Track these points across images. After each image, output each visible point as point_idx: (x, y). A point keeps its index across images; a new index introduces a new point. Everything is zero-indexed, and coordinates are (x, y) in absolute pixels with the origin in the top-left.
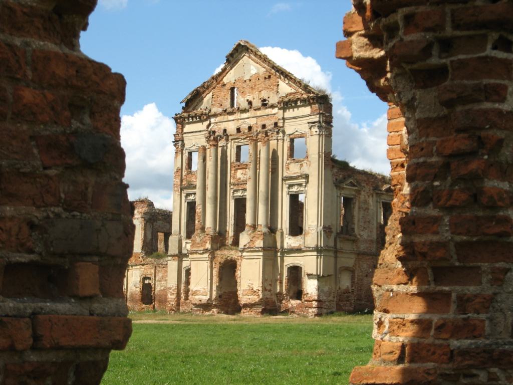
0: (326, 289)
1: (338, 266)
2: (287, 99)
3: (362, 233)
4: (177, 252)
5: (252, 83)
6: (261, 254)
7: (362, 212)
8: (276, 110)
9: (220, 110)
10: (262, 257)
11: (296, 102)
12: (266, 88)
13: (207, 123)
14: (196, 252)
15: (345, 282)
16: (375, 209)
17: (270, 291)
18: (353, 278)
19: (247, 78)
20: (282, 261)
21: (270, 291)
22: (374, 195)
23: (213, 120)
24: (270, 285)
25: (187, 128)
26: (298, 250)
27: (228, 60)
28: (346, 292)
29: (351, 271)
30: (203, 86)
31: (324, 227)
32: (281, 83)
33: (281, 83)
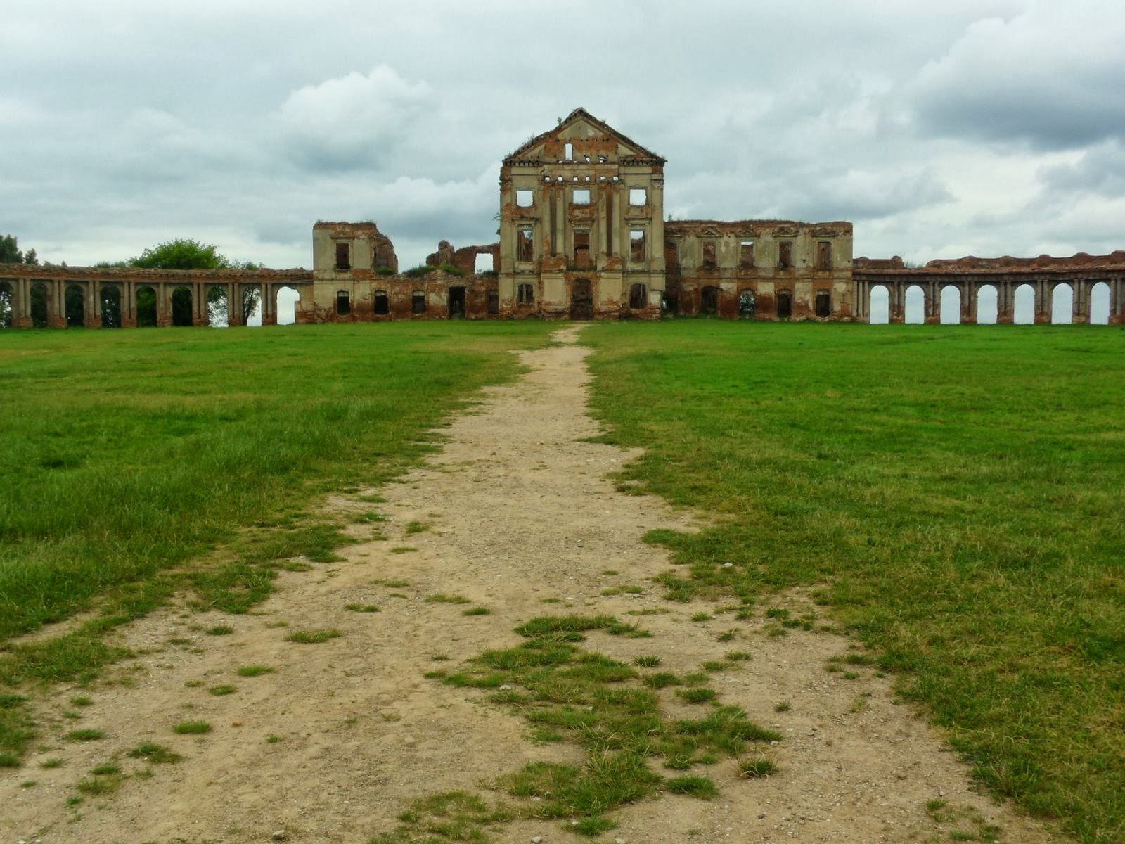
2: (629, 159)
4: (511, 271)
5: (590, 143)
8: (616, 166)
9: (555, 160)
11: (638, 163)
12: (606, 148)
13: (540, 169)
14: (551, 272)
19: (584, 138)
23: (546, 167)
25: (515, 170)
26: (642, 272)
32: (620, 146)
33: (620, 146)
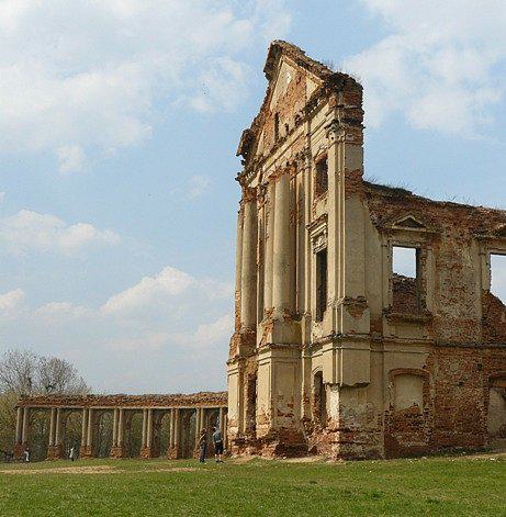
0: (361, 408)
1: (387, 368)
3: (444, 309)
6: (269, 354)
7: (444, 274)
10: (270, 360)
15: (409, 396)
16: (476, 267)
17: (289, 415)
18: (426, 388)
20: (309, 362)
21: (289, 415)
22: (474, 242)
24: (292, 406)
27: (268, 77)
28: (412, 414)
29: (422, 376)
30: (254, 124)
31: (346, 300)
